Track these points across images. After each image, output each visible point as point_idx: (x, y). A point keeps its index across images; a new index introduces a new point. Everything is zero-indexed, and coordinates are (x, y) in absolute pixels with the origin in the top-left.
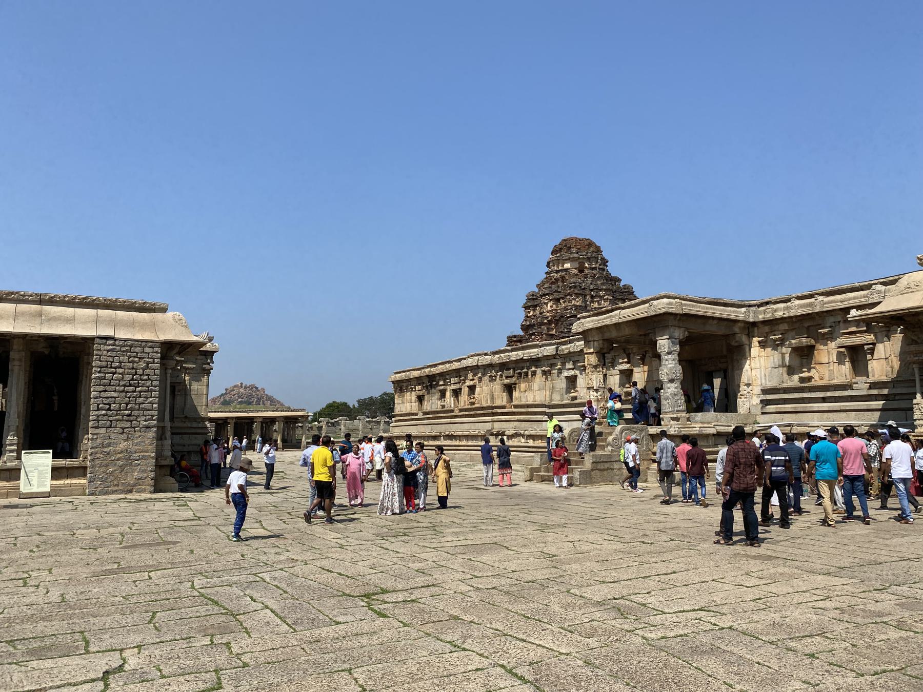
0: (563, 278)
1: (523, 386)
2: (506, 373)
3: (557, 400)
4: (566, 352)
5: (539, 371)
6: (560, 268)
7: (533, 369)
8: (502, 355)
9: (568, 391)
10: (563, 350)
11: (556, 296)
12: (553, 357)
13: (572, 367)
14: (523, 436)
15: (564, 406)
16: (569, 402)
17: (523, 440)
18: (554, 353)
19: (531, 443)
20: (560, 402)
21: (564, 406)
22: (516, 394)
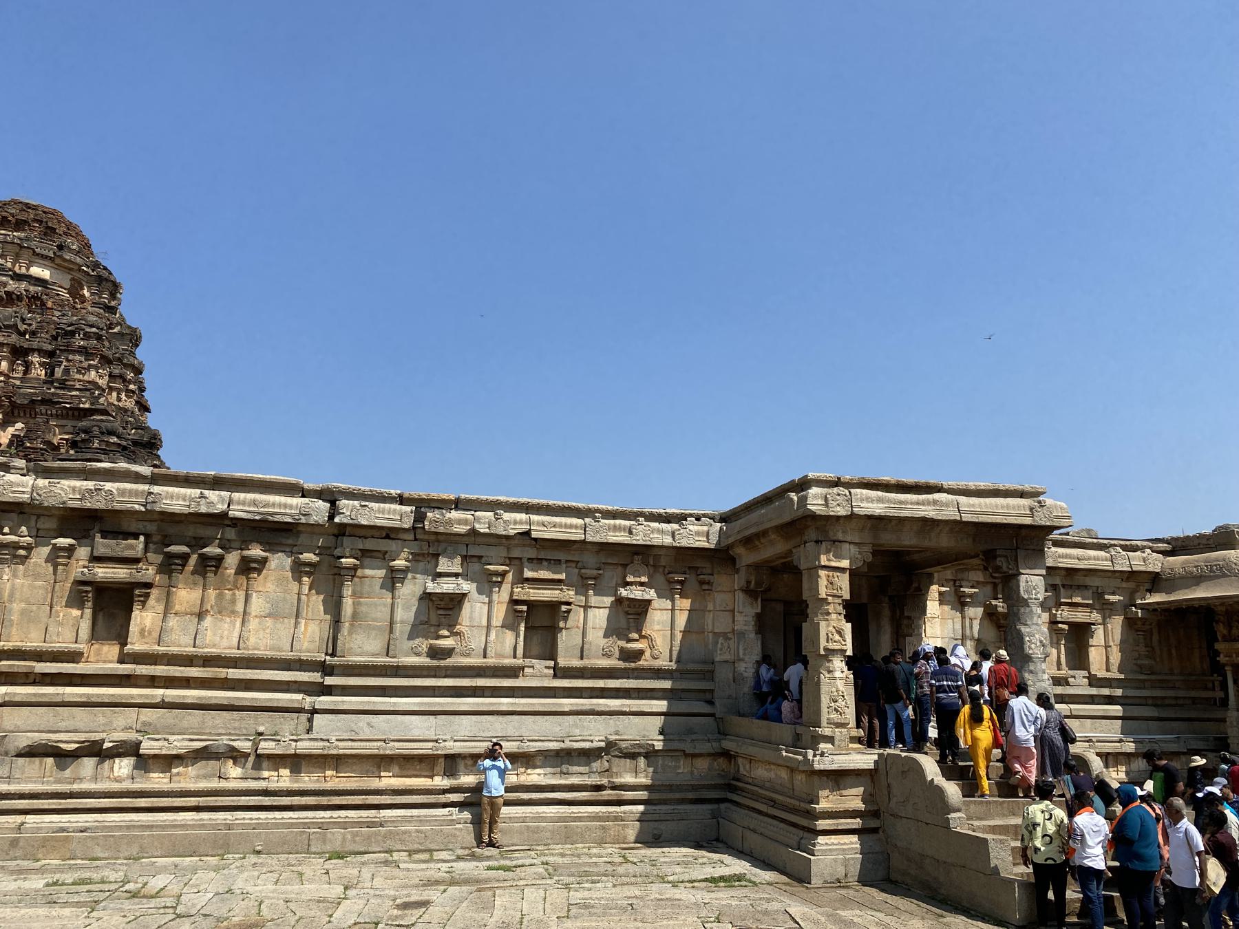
0: (35, 298)
1: (186, 595)
2: (103, 546)
3: (362, 647)
4: (462, 529)
5: (279, 562)
6: (23, 271)
7: (256, 551)
8: (108, 486)
9: (421, 627)
10: (450, 522)
11: (14, 339)
12: (389, 533)
13: (457, 569)
14: (235, 756)
15: (397, 671)
16: (426, 661)
17: (234, 771)
18: (408, 523)
19: (282, 779)
20: (382, 660)
21: (397, 671)
22: (143, 619)
